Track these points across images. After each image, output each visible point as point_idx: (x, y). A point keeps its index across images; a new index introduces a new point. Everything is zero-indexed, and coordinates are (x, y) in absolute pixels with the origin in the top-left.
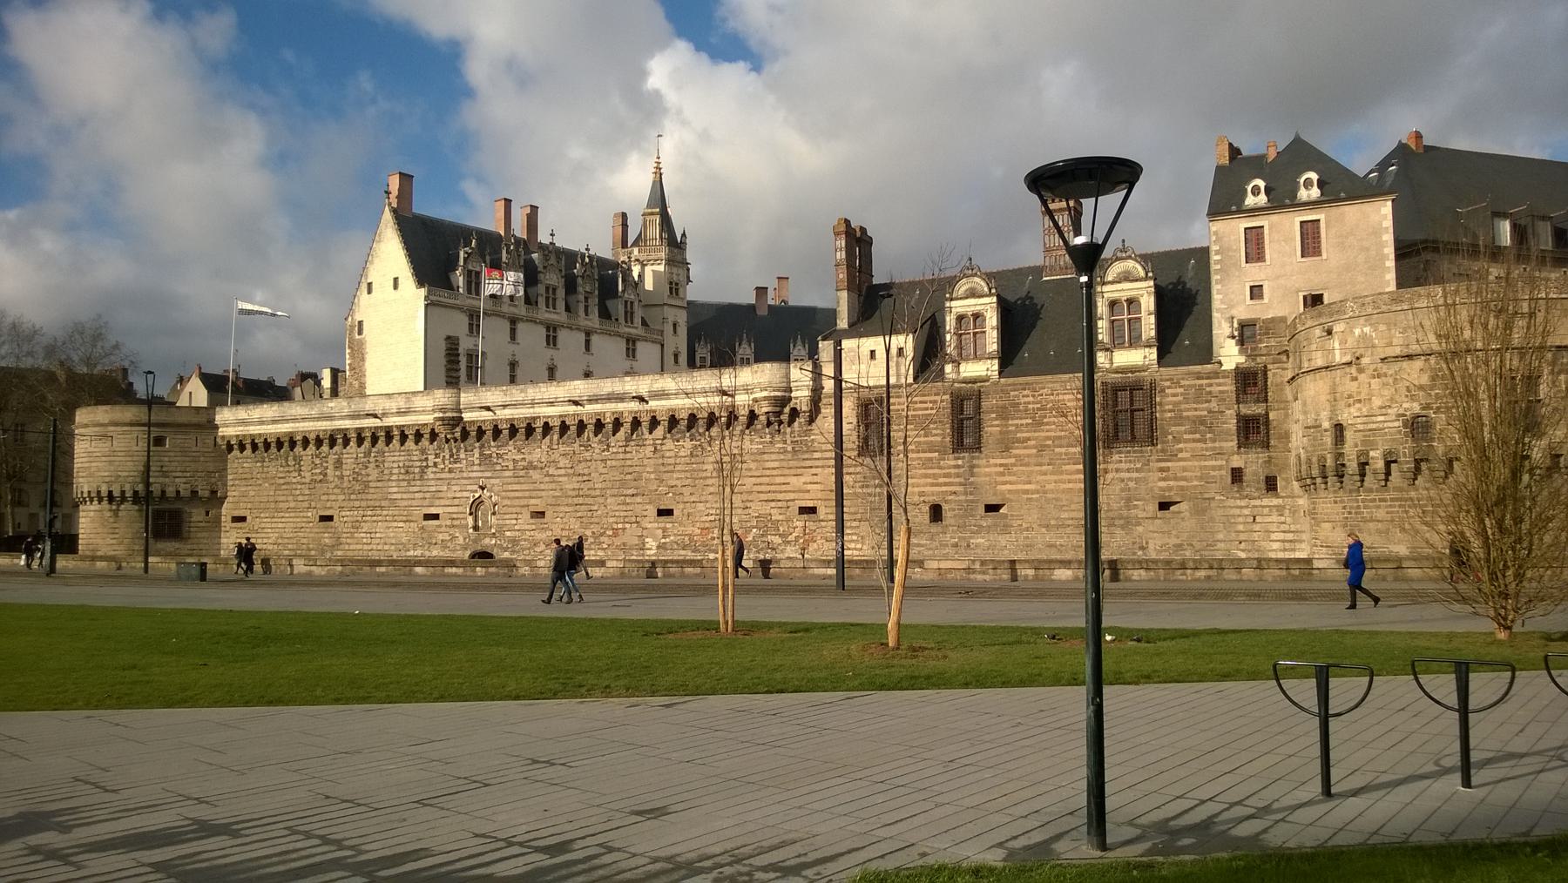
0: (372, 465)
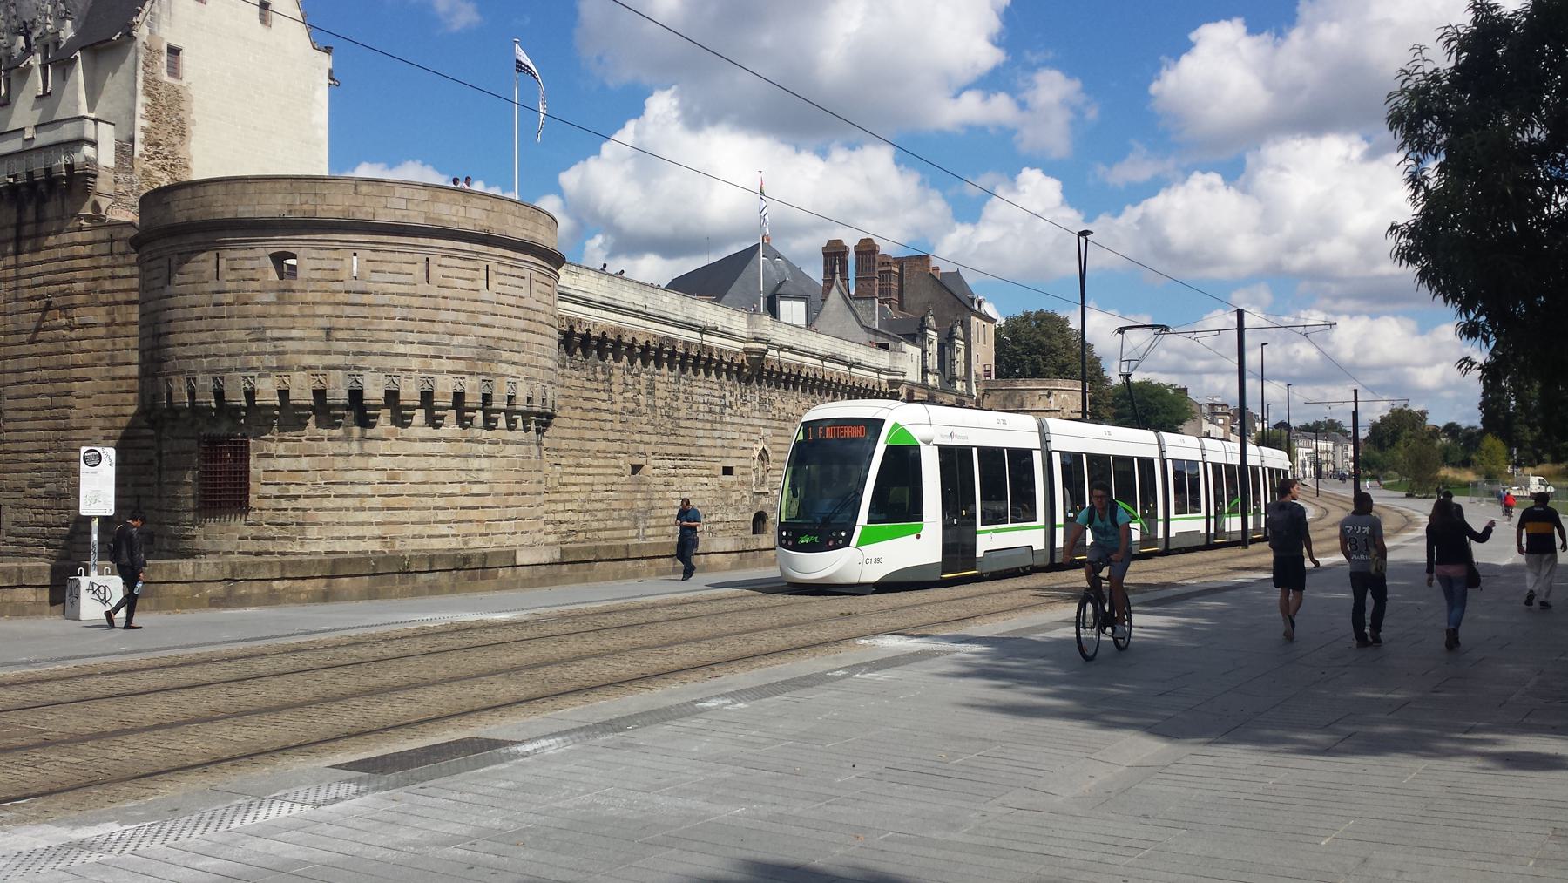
0: (682, 396)
